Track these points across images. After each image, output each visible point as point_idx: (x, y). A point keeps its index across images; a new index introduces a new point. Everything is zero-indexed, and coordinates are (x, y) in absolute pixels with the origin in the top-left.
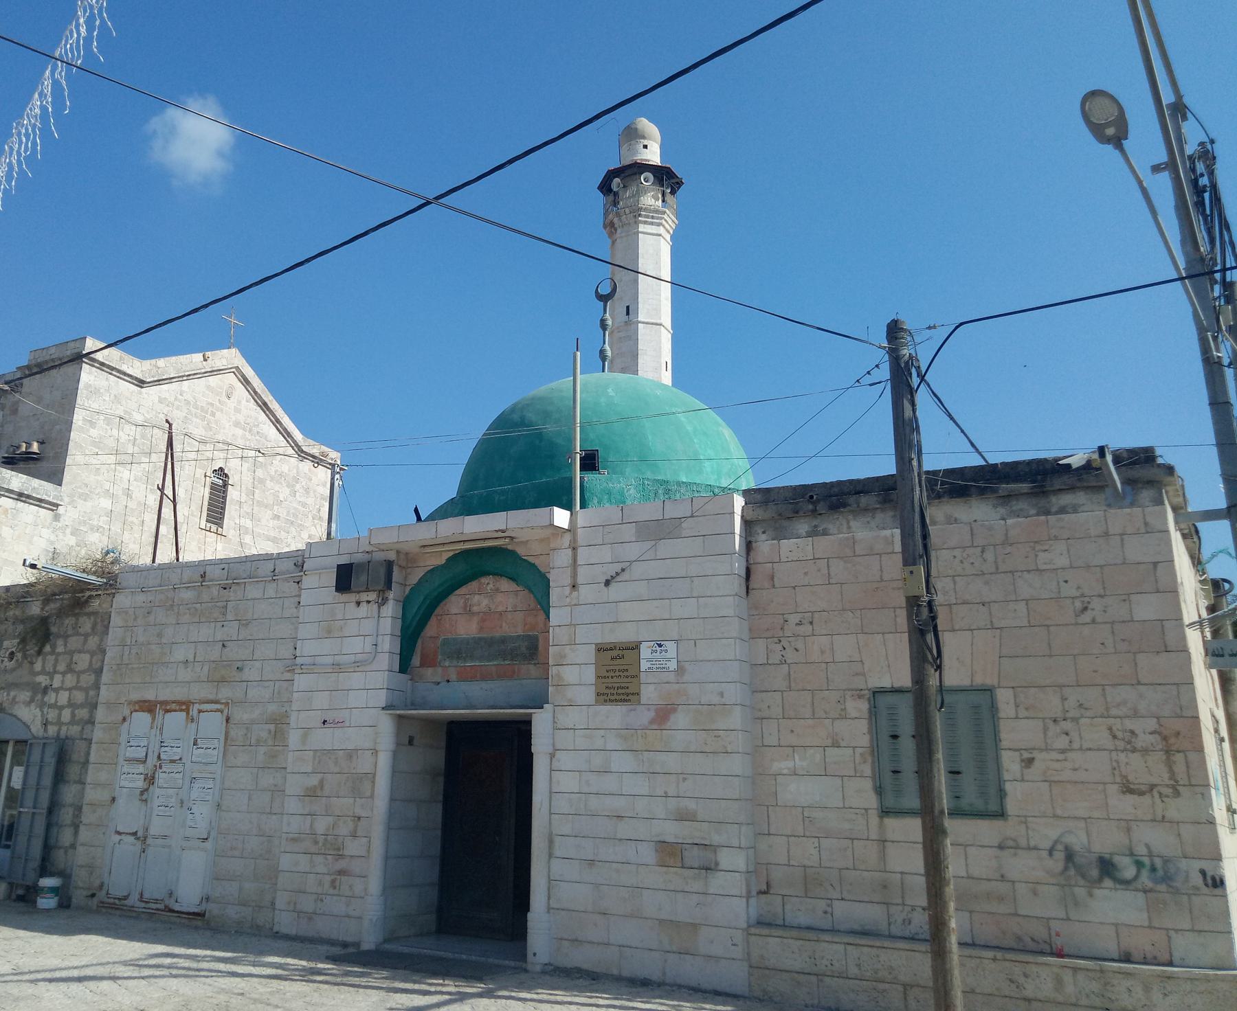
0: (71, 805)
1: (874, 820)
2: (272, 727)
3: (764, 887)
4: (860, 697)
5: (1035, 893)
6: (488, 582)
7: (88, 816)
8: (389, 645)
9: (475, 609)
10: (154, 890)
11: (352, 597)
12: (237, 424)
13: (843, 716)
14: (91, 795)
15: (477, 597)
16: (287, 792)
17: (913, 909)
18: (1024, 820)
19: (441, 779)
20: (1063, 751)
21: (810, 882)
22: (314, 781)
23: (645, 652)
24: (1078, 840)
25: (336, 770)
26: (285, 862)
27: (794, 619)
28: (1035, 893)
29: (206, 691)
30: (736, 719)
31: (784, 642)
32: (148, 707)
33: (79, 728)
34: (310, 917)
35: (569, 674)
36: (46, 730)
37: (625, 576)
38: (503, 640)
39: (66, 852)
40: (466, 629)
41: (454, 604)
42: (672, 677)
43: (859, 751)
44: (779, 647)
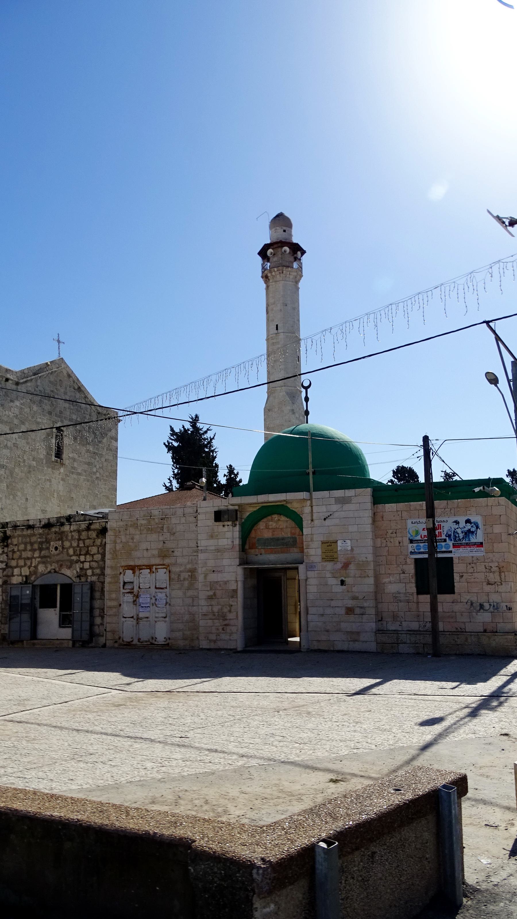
2: (190, 574)
3: (380, 619)
5: (462, 615)
6: (276, 517)
10: (145, 636)
11: (221, 523)
13: (406, 563)
14: (108, 603)
18: (460, 594)
20: (472, 573)
22: (211, 593)
23: (339, 543)
24: (474, 599)
25: (221, 588)
26: (202, 623)
28: (462, 615)
29: (157, 561)
32: (133, 568)
34: (215, 641)
35: (312, 552)
37: (330, 517)
38: (283, 539)
40: (267, 535)
41: (262, 525)
42: (349, 552)
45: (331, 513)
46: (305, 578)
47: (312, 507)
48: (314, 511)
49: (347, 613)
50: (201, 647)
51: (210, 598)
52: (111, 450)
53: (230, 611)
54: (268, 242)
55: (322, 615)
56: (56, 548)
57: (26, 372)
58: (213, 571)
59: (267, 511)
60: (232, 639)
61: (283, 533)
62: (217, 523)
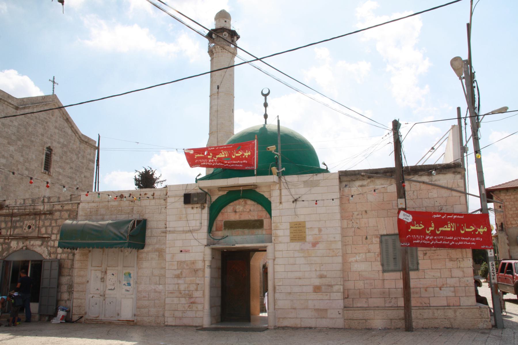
0: (66, 284)
1: (381, 274)
3: (347, 297)
4: (377, 237)
5: (426, 290)
7: (76, 288)
8: (206, 223)
11: (190, 206)
12: (56, 127)
14: (76, 280)
15: (238, 206)
16: (167, 276)
17: (392, 298)
18: (424, 271)
19: (220, 270)
21: (361, 294)
22: (178, 272)
26: (168, 301)
27: (356, 213)
28: (426, 290)
30: (339, 245)
31: (353, 221)
33: (67, 255)
34: (180, 318)
35: (280, 233)
36: (50, 256)
37: (300, 199)
39: (66, 302)
41: (229, 209)
43: (376, 254)
44: (351, 222)
45: (300, 196)
46: (273, 258)
47: (280, 190)
48: (283, 194)
50: (166, 324)
51: (178, 277)
52: (89, 169)
53: (197, 290)
54: (214, 28)
55: (290, 293)
56: (30, 227)
57: (25, 100)
58: (181, 251)
59: (234, 195)
60: (197, 316)
62: (187, 206)
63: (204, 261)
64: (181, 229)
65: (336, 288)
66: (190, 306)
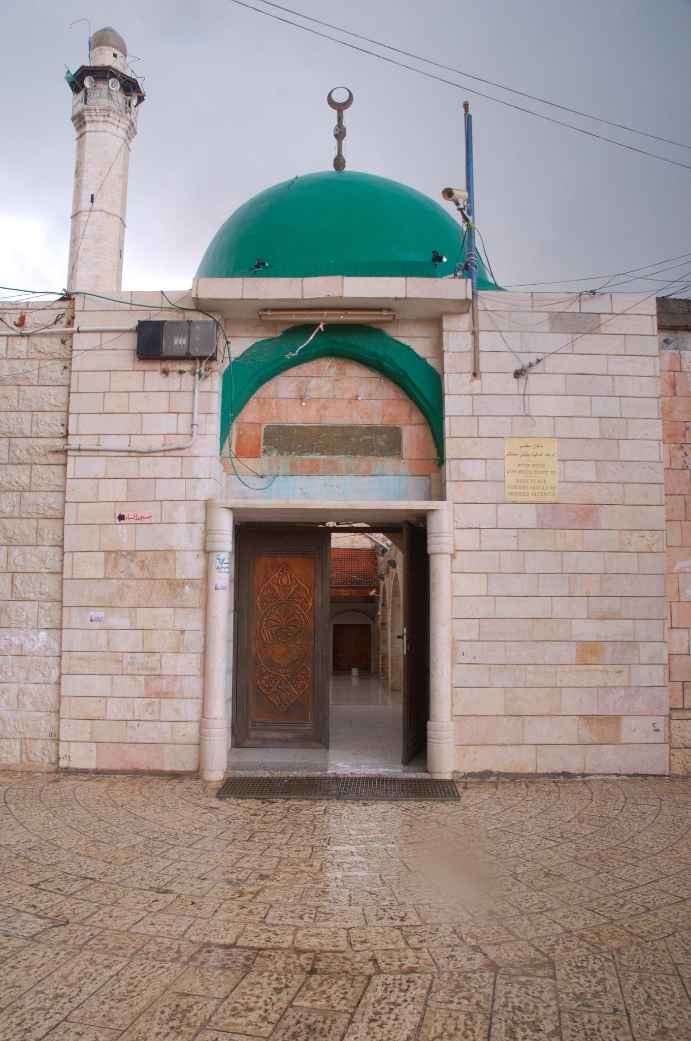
9: (314, 394)
15: (314, 382)
25: (146, 574)
37: (538, 368)
45: (540, 356)
47: (474, 333)
49: (582, 661)
50: (63, 763)
58: (121, 517)
61: (355, 414)
63: (207, 552)
64: (121, 443)
65: (646, 652)
66: (150, 704)
